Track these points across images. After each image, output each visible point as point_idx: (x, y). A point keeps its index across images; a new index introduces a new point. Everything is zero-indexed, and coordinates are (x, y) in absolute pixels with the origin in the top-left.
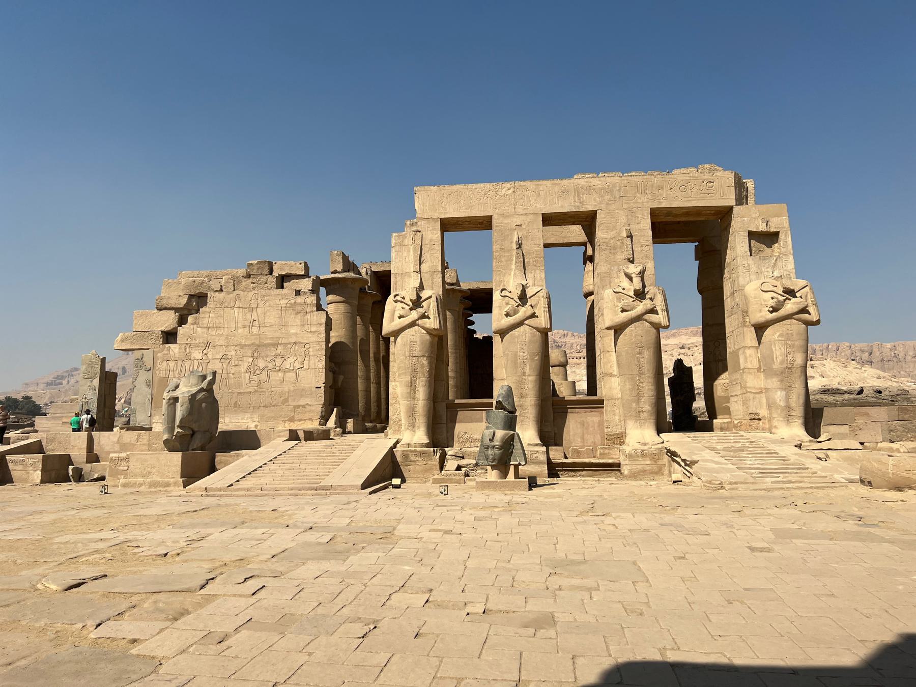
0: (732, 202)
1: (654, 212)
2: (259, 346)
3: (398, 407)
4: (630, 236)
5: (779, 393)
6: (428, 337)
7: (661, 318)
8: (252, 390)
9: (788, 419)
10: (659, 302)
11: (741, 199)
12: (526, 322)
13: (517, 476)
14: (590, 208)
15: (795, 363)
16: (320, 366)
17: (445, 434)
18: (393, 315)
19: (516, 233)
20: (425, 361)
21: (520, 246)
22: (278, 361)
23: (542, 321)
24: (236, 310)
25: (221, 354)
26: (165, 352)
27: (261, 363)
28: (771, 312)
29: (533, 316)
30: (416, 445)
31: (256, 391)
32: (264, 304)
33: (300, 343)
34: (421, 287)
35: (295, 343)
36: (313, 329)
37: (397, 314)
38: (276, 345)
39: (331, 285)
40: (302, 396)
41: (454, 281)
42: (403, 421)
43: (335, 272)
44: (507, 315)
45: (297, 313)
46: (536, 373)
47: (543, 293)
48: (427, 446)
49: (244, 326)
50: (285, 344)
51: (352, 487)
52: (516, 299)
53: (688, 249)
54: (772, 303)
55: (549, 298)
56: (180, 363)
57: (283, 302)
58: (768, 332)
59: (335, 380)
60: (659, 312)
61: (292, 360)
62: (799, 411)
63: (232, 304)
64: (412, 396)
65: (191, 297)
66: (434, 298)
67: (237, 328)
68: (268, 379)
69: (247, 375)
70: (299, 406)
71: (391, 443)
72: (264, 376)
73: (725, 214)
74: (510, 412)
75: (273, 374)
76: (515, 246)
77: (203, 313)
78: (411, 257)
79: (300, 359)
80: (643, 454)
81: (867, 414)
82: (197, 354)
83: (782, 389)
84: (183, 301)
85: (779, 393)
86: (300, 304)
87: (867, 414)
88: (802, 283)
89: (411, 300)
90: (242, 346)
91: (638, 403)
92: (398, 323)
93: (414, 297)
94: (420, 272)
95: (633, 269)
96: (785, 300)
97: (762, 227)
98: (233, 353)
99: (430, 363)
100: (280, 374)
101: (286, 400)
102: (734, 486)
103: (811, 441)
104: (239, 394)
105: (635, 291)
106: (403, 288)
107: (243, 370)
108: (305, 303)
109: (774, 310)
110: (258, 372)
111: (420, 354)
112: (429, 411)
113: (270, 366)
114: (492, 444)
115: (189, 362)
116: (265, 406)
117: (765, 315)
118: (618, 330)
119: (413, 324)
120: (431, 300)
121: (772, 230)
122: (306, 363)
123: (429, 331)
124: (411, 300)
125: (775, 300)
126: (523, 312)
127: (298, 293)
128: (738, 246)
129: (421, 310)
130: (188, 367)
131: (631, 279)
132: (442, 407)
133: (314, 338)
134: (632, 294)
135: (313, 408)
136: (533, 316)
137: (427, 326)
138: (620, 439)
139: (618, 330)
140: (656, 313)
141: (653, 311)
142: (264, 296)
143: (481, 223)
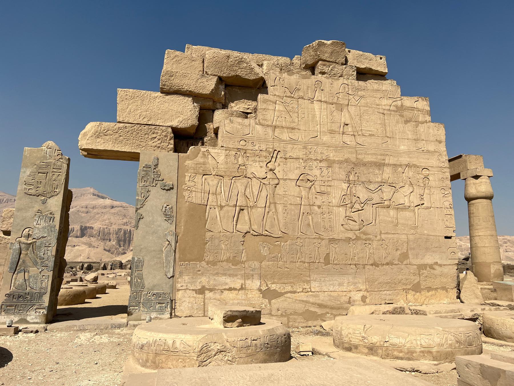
8: (350, 235)
16: (447, 204)
24: (316, 106)
25: (298, 172)
26: (200, 159)
31: (358, 238)
33: (415, 166)
36: (431, 148)
38: (380, 165)
40: (427, 249)
45: (406, 122)
49: (332, 132)
61: (407, 189)
75: (382, 212)
77: (265, 101)
82: (257, 168)
90: (330, 163)
98: (317, 172)
101: (405, 256)
104: (332, 240)
107: (335, 201)
110: (357, 206)
113: (376, 198)
115: (245, 180)
116: (375, 264)
130: (241, 189)
135: (445, 270)
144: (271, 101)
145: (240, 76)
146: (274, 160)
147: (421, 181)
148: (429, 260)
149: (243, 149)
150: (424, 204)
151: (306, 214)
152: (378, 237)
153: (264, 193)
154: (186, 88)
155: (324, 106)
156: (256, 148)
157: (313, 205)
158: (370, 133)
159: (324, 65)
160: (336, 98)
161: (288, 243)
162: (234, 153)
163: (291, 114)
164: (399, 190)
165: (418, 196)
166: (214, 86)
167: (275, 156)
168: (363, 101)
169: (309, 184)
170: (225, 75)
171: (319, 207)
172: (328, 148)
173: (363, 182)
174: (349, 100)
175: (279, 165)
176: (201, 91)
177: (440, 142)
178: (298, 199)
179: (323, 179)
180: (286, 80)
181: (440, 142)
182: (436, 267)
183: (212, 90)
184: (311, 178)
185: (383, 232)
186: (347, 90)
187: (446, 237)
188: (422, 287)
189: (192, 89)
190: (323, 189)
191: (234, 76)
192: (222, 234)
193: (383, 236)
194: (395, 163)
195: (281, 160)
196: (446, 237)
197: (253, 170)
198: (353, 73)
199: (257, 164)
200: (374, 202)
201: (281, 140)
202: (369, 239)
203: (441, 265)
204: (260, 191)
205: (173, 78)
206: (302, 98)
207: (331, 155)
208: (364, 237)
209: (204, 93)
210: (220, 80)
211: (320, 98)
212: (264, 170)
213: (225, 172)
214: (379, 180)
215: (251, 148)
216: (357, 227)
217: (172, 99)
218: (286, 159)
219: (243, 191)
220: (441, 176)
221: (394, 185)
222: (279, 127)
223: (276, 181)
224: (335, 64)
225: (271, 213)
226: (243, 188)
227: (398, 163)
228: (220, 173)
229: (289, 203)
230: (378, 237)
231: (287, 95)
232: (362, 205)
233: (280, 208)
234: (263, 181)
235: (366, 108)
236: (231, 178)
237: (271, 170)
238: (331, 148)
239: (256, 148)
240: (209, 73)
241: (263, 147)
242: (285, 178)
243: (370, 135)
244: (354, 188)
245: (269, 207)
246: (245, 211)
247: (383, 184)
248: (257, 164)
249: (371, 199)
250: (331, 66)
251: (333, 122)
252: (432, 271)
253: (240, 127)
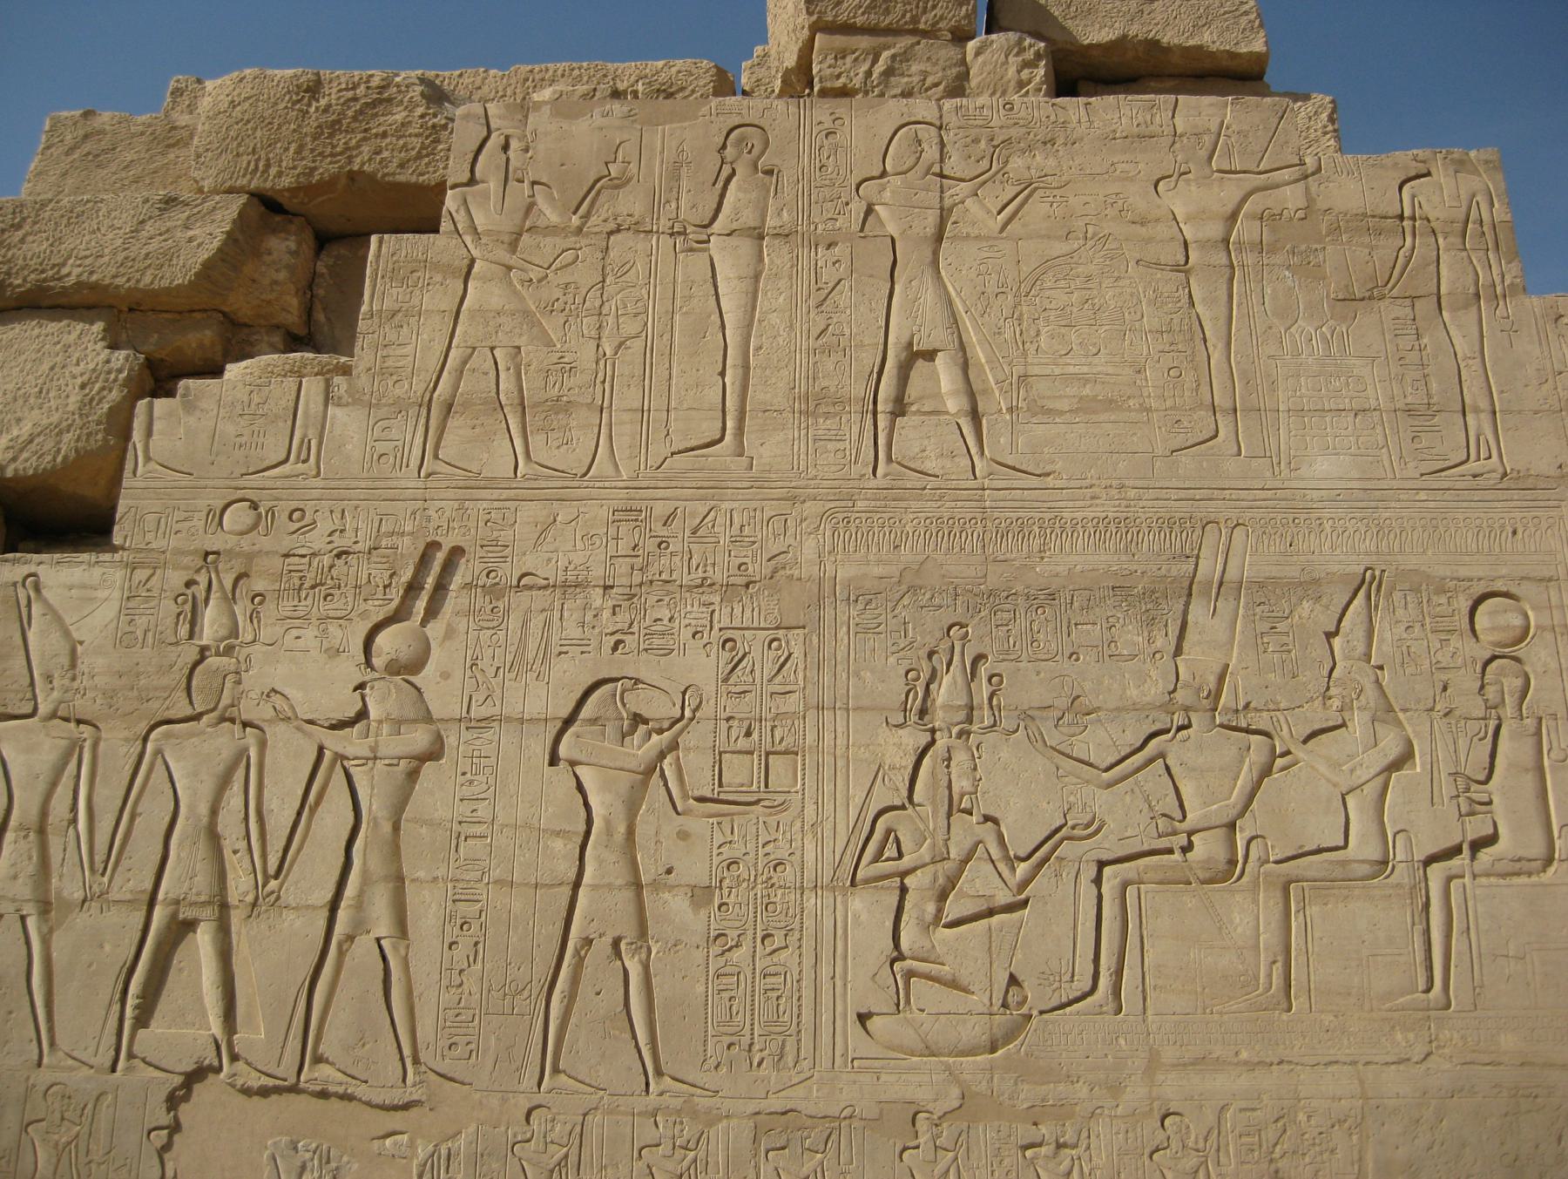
2: (994, 599)
8: (921, 1084)
22: (1207, 771)
25: (572, 673)
27: (1017, 787)
32: (1012, 211)
35: (1365, 584)
49: (813, 404)
50: (1266, 593)
56: (117, 746)
57: (1192, 204)
61: (1360, 749)
63: (691, 204)
65: (269, 207)
67: (737, 419)
68: (1107, 977)
69: (866, 912)
72: (1056, 928)
75: (1166, 918)
82: (303, 667)
84: (204, 236)
86: (1369, 224)
100: (1247, 914)
107: (820, 851)
110: (982, 883)
113: (1125, 817)
115: (221, 743)
122: (1507, 795)
130: (194, 793)
142: (1002, 147)
144: (437, 266)
145: (371, 177)
146: (421, 605)
147: (1466, 681)
149: (230, 553)
150: (1492, 839)
151: (603, 945)
152: (1135, 1093)
153: (333, 817)
154: (73, 273)
155: (775, 256)
156: (316, 539)
157: (656, 885)
158: (1087, 391)
159: (842, 54)
160: (858, 207)
161: (462, 1141)
162: (176, 579)
163: (551, 326)
164: (1299, 752)
165: (1447, 789)
166: (216, 244)
167: (430, 581)
168: (1037, 209)
169: (642, 749)
170: (286, 182)
171: (701, 895)
172: (785, 506)
173: (1027, 716)
174: (944, 215)
175: (450, 633)
176: (147, 279)
178: (558, 844)
179: (743, 707)
180: (541, 147)
183: (208, 266)
184: (659, 707)
185: (1169, 1054)
186: (931, 153)
189: (104, 273)
190: (738, 772)
191: (334, 179)
192: (43, 1077)
193: (1171, 1087)
194: (1274, 571)
195: (464, 601)
197: (278, 674)
198: (1025, 74)
199: (310, 633)
200: (1106, 845)
201: (476, 483)
202: (1062, 1110)
204: (306, 805)
205: (20, 233)
206: (637, 228)
207: (809, 549)
208: (1027, 1094)
209: (165, 283)
210: (269, 207)
211: (749, 218)
212: (349, 669)
213: (110, 694)
214: (1155, 690)
215: (287, 543)
216: (974, 1030)
217: (11, 334)
218: (495, 591)
219: (204, 809)
221: (1261, 721)
222: (466, 405)
223: (419, 738)
224: (908, 41)
225: (364, 944)
226: (207, 788)
227: (1293, 572)
228: (82, 706)
229: (496, 874)
230: (1135, 1093)
231: (541, 223)
232: (1022, 868)
233: (426, 908)
234: (335, 742)
235: (1061, 248)
236: (143, 727)
237: (394, 668)
238: (811, 508)
239: (316, 539)
240: (207, 185)
241: (360, 532)
242: (485, 711)
243: (1086, 407)
244: (960, 757)
245: (359, 904)
246: (203, 940)
247: (1179, 719)
248: (310, 633)
249: (1093, 828)
250: (886, 54)
251: (828, 350)
253: (230, 429)
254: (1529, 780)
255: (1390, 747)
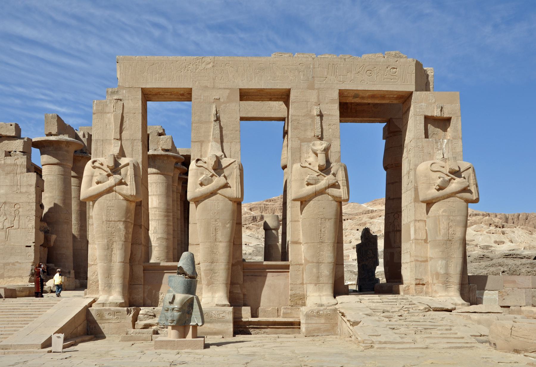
0: (412, 88)
1: (342, 93)
3: (96, 269)
4: (321, 115)
5: (440, 262)
6: (125, 203)
7: (341, 192)
9: (446, 285)
10: (341, 176)
11: (423, 84)
12: (219, 192)
13: (195, 336)
14: (286, 86)
15: (456, 236)
16: (30, 226)
17: (142, 295)
18: (91, 180)
19: (214, 106)
20: (121, 226)
21: (218, 119)
23: (234, 191)
28: (438, 190)
29: (226, 186)
30: (111, 304)
34: (122, 153)
35: (5, 203)
36: (24, 190)
37: (95, 179)
39: (44, 147)
41: (169, 147)
42: (100, 282)
43: (50, 134)
44: (201, 184)
46: (227, 239)
47: (236, 166)
48: (121, 305)
51: (32, 346)
52: (210, 168)
53: (379, 127)
54: (439, 181)
55: (241, 170)
58: (434, 208)
59: (47, 239)
60: (341, 187)
62: (455, 279)
64: (108, 259)
66: (131, 166)
70: (8, 264)
71: (87, 302)
73: (405, 99)
74: (190, 277)
76: (213, 118)
78: (112, 126)
79: (10, 218)
80: (318, 315)
81: (514, 282)
83: (442, 258)
85: (440, 262)
87: (514, 282)
88: (467, 164)
89: (108, 167)
91: (318, 268)
92: (95, 188)
93: (112, 164)
94: (121, 139)
95: (320, 146)
96: (450, 180)
97: (436, 113)
99: (126, 228)
102: (383, 345)
103: (463, 304)
105: (319, 166)
106: (102, 155)
108: (15, 165)
109: (440, 189)
111: (117, 219)
112: (124, 273)
114: (172, 306)
117: (433, 193)
118: (304, 201)
119: (110, 190)
120: (129, 167)
121: (446, 115)
123: (126, 198)
124: (108, 167)
125: (441, 179)
126: (219, 181)
127: (8, 154)
128: (414, 128)
129: (118, 177)
131: (317, 155)
132: (139, 270)
133: (24, 199)
134: (317, 169)
136: (226, 186)
137: (124, 192)
138: (299, 300)
139: (304, 201)
140: (338, 187)
141: (335, 186)
143: (182, 95)
147: (13, 212)
148: (12, 260)
177: (31, 186)
181: (31, 186)
182: (16, 264)
187: (27, 246)
188: (5, 276)
196: (27, 246)
203: (20, 263)
220: (28, 208)
252: (13, 266)
254: (18, 221)
255: (5, 218)
